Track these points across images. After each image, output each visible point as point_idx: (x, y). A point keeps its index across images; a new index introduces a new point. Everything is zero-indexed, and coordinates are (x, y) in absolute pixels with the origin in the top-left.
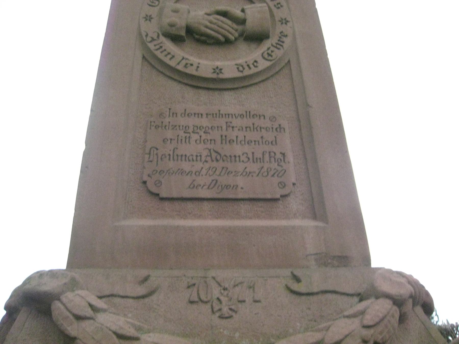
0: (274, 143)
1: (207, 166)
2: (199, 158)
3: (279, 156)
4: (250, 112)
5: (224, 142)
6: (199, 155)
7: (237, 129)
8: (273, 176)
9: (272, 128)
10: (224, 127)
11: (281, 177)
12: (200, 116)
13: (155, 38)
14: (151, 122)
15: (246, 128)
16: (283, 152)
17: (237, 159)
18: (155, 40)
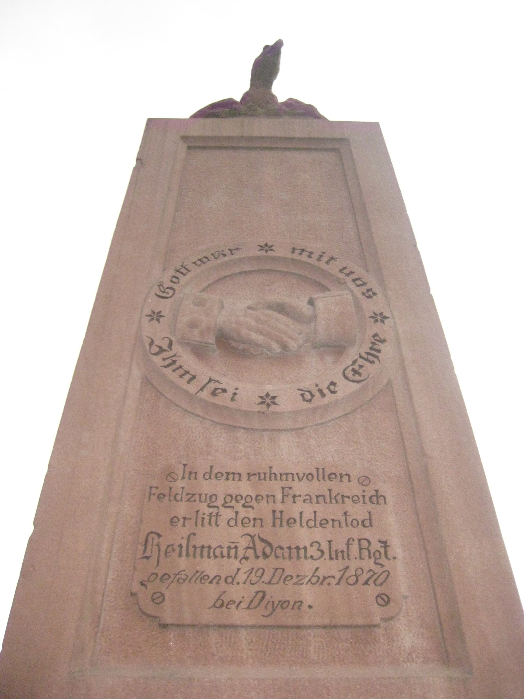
0: (367, 523)
1: (246, 566)
2: (233, 552)
3: (376, 546)
4: (323, 469)
5: (278, 522)
6: (233, 545)
7: (301, 499)
8: (366, 583)
9: (364, 496)
10: (279, 496)
11: (382, 584)
12: (237, 476)
13: (165, 347)
14: (151, 488)
15: (317, 497)
16: (384, 540)
17: (302, 552)
18: (165, 350)
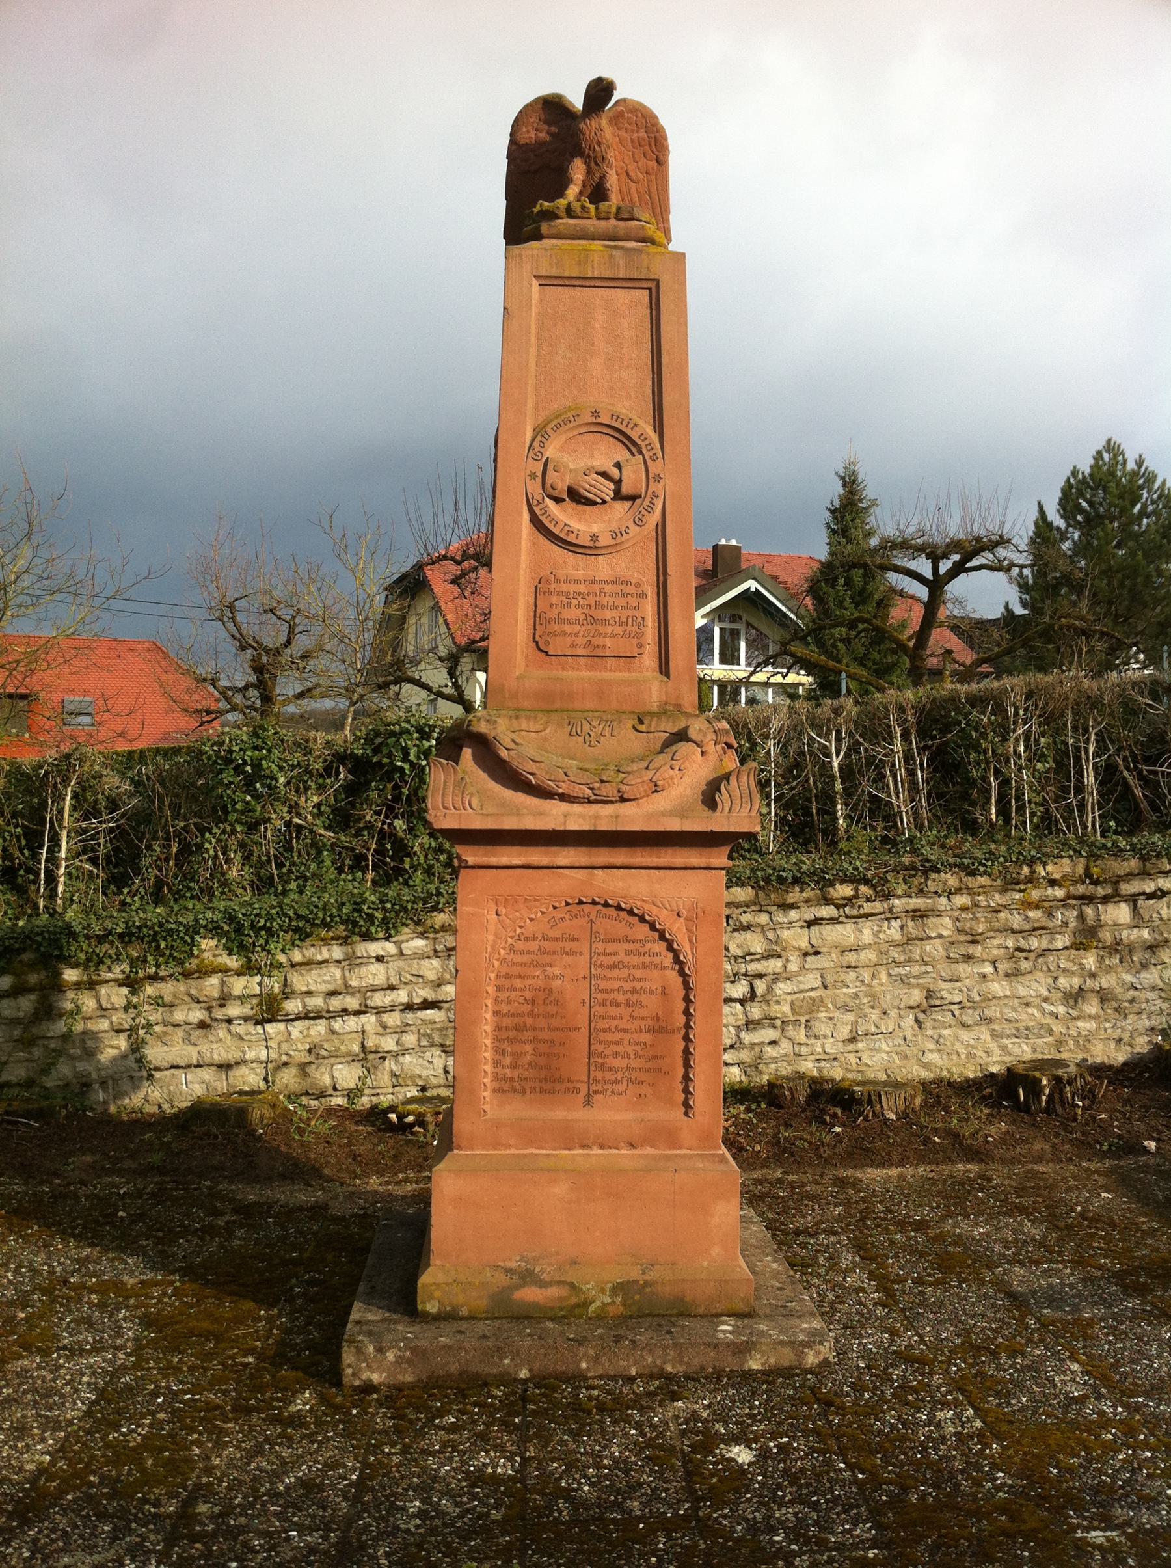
1: (584, 628)
3: (640, 620)
